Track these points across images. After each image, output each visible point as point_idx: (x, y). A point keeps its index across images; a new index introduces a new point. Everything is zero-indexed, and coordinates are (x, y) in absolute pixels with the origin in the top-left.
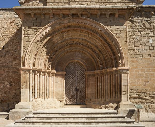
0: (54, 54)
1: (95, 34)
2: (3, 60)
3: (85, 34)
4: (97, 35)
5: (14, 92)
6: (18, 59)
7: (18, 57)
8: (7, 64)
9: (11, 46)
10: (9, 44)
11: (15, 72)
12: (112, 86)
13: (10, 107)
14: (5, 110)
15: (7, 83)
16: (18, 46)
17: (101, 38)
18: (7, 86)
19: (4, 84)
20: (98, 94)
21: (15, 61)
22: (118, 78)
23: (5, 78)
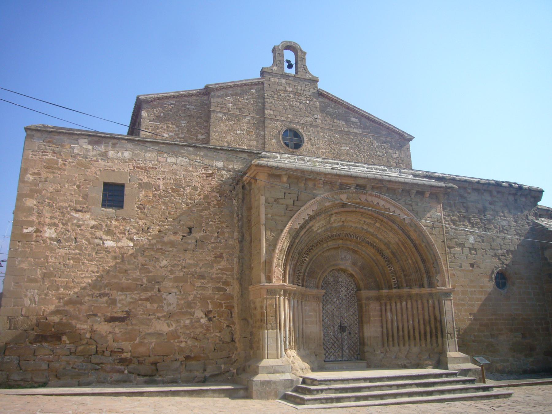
0: (308, 254)
1: (390, 223)
2: (189, 259)
3: (368, 221)
4: (394, 225)
5: (217, 336)
6: (226, 259)
7: (224, 255)
8: (198, 270)
9: (209, 229)
10: (204, 224)
11: (219, 289)
12: (422, 322)
13: (208, 370)
14: (196, 380)
15: (199, 314)
16: (225, 230)
17: (400, 232)
18: (199, 321)
19: (192, 317)
20: (388, 337)
21: (219, 262)
22: (434, 308)
23: (194, 303)
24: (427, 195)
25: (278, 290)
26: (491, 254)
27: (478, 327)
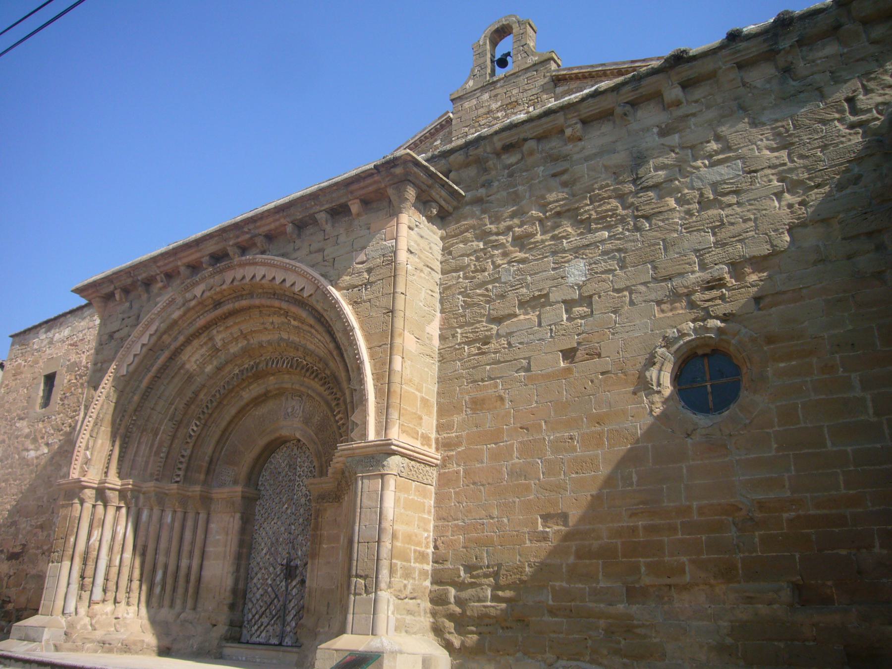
3: (277, 320)
24: (355, 207)
25: (77, 490)
26: (653, 296)
27: (571, 559)
